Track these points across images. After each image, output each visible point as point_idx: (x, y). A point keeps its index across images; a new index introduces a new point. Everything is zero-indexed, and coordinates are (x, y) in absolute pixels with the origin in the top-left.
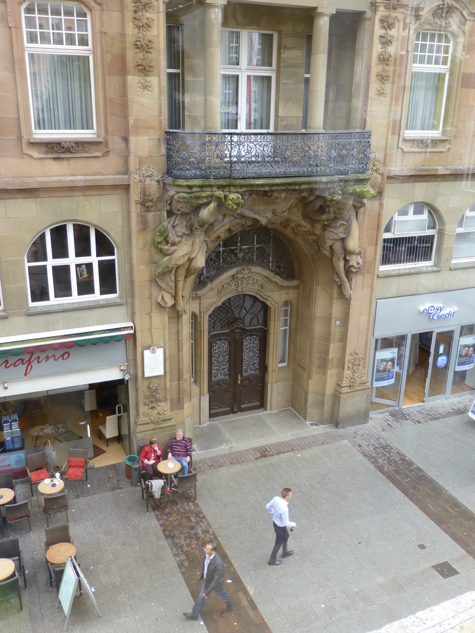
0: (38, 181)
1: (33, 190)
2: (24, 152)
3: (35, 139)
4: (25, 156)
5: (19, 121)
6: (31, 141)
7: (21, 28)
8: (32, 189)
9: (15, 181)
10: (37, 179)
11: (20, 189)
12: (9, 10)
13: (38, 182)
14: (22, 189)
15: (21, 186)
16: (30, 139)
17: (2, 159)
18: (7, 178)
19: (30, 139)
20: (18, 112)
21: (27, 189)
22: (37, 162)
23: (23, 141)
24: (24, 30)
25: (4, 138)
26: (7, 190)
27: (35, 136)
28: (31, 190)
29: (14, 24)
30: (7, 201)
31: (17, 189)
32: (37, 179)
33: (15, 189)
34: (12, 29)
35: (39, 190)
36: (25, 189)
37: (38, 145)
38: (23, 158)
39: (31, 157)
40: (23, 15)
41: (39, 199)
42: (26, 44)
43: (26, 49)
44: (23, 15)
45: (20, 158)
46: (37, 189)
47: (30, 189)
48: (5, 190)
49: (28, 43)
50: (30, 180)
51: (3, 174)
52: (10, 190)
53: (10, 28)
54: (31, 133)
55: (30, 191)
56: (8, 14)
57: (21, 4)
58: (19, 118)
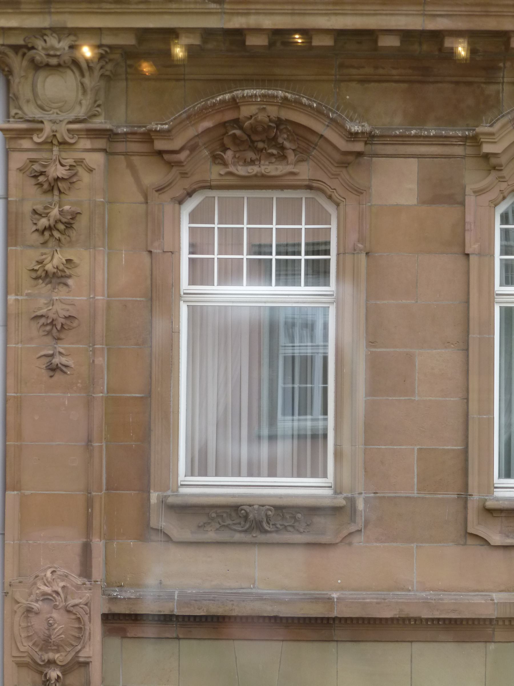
0: (496, 601)
1: (481, 623)
2: (470, 530)
3: (498, 499)
4: (470, 541)
5: (466, 460)
6: (490, 504)
7: (493, 255)
8: (479, 619)
9: (442, 599)
10: (494, 595)
11: (450, 620)
12: (469, 218)
13: (495, 603)
14: (456, 620)
15: (454, 611)
16: (486, 500)
17: (417, 546)
18: (424, 590)
19: (486, 500)
20: (467, 437)
21: (468, 620)
22: (499, 554)
23: (470, 505)
24: (498, 257)
25: (428, 496)
26: (421, 619)
27: (499, 493)
28: (476, 623)
29: (476, 246)
30: (416, 645)
31: (444, 619)
32: (494, 595)
33: (439, 619)
34: (471, 257)
35: (494, 622)
36: (462, 620)
37: (503, 515)
38: (465, 544)
39: (485, 542)
40: (498, 227)
41: (492, 646)
42: (498, 288)
43: (498, 299)
44: (498, 227)
45: (458, 544)
46: (491, 620)
47: (473, 620)
48: (415, 619)
49: (501, 285)
50: (478, 599)
51: (415, 581)
52: (427, 620)
53: (468, 255)
54: (490, 487)
55: (473, 623)
56: (467, 227)
57: (496, 205)
58: (466, 451)
